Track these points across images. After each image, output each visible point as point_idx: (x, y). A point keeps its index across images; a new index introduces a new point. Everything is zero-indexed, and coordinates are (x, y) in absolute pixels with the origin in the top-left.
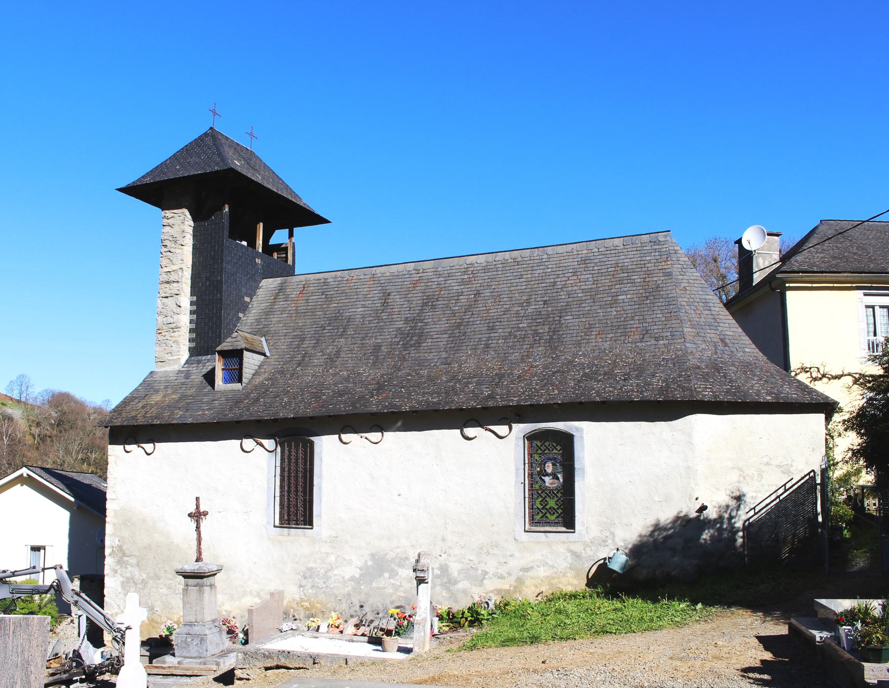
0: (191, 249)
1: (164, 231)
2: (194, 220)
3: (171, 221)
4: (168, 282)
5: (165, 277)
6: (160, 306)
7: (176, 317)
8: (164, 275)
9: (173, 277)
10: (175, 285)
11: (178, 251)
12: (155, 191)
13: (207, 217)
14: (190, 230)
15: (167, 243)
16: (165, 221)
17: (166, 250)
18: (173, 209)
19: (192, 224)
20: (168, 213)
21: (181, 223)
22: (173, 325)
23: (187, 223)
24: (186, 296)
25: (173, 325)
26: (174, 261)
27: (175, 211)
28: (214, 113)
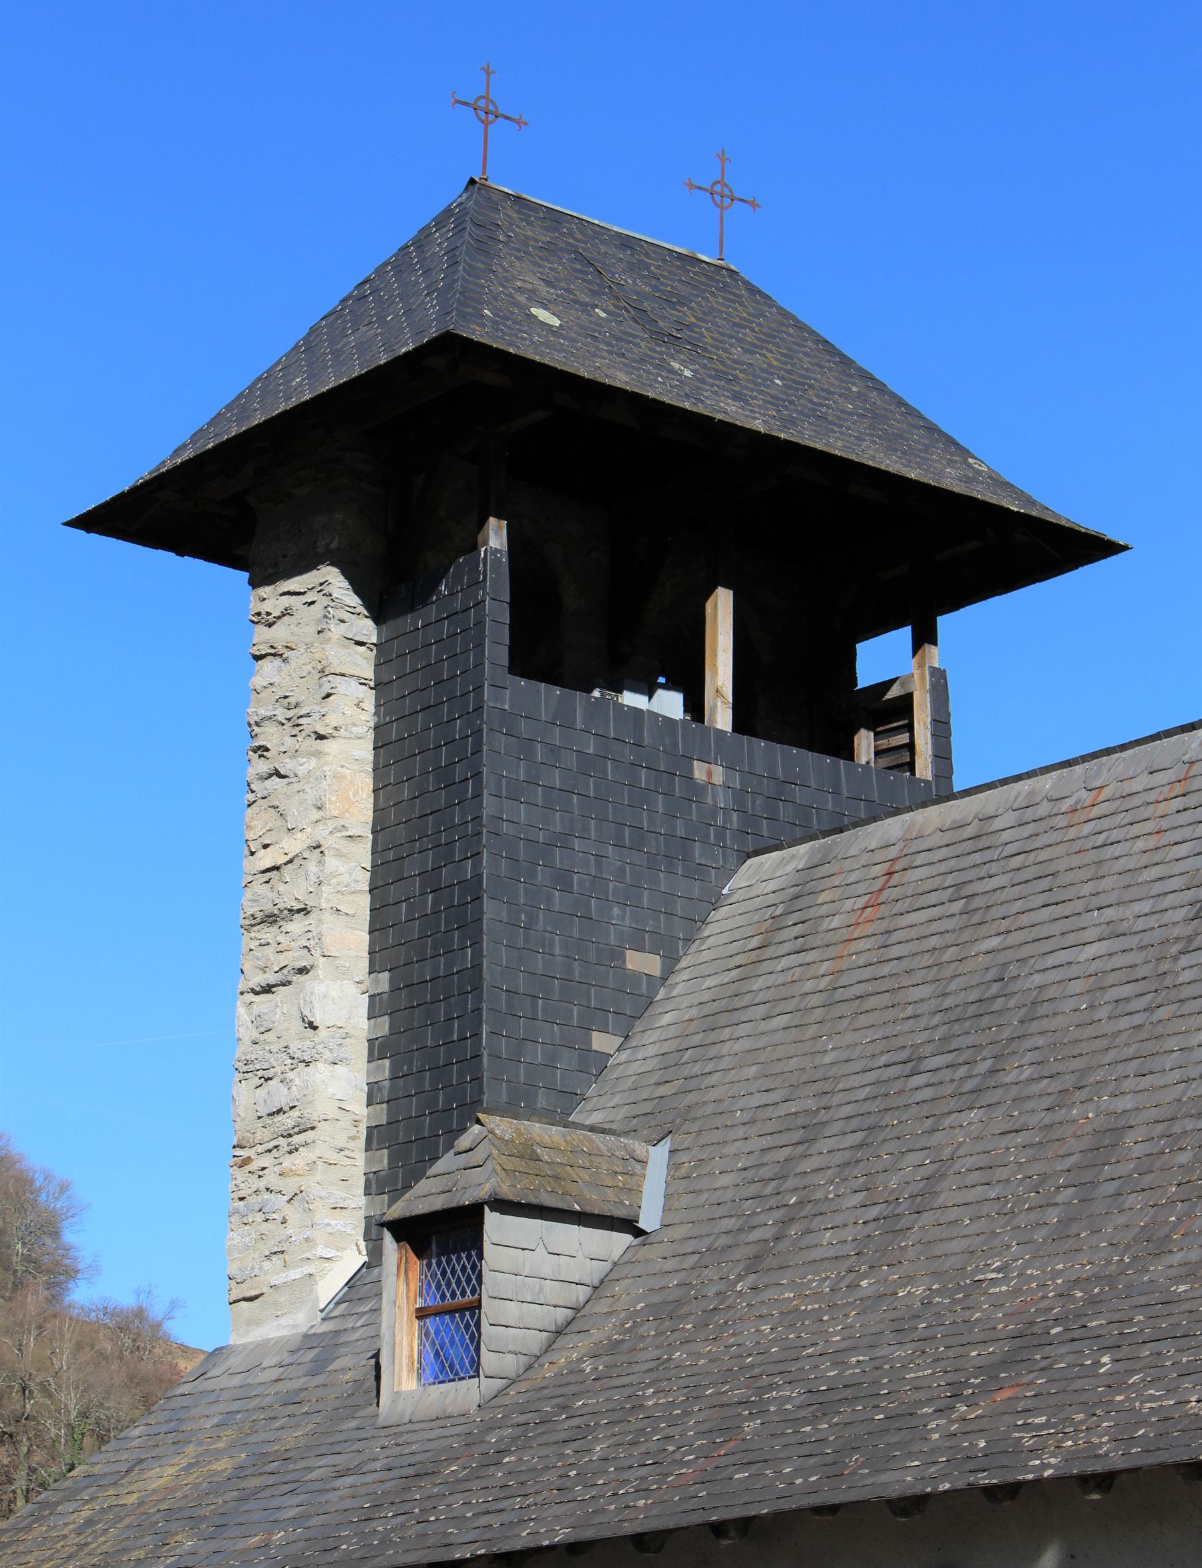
0: (364, 750)
1: (258, 681)
2: (378, 611)
3: (279, 634)
4: (270, 919)
5: (260, 897)
6: (246, 1032)
7: (299, 1077)
8: (259, 888)
9: (291, 891)
10: (296, 926)
11: (304, 766)
12: (214, 506)
13: (418, 598)
14: (364, 664)
15: (270, 736)
16: (262, 635)
17: (263, 767)
18: (289, 575)
19: (367, 629)
20: (271, 598)
21: (319, 641)
22: (288, 1121)
23: (337, 630)
24: (342, 973)
25: (288, 1121)
26: (293, 811)
27: (294, 584)
28: (487, 112)
